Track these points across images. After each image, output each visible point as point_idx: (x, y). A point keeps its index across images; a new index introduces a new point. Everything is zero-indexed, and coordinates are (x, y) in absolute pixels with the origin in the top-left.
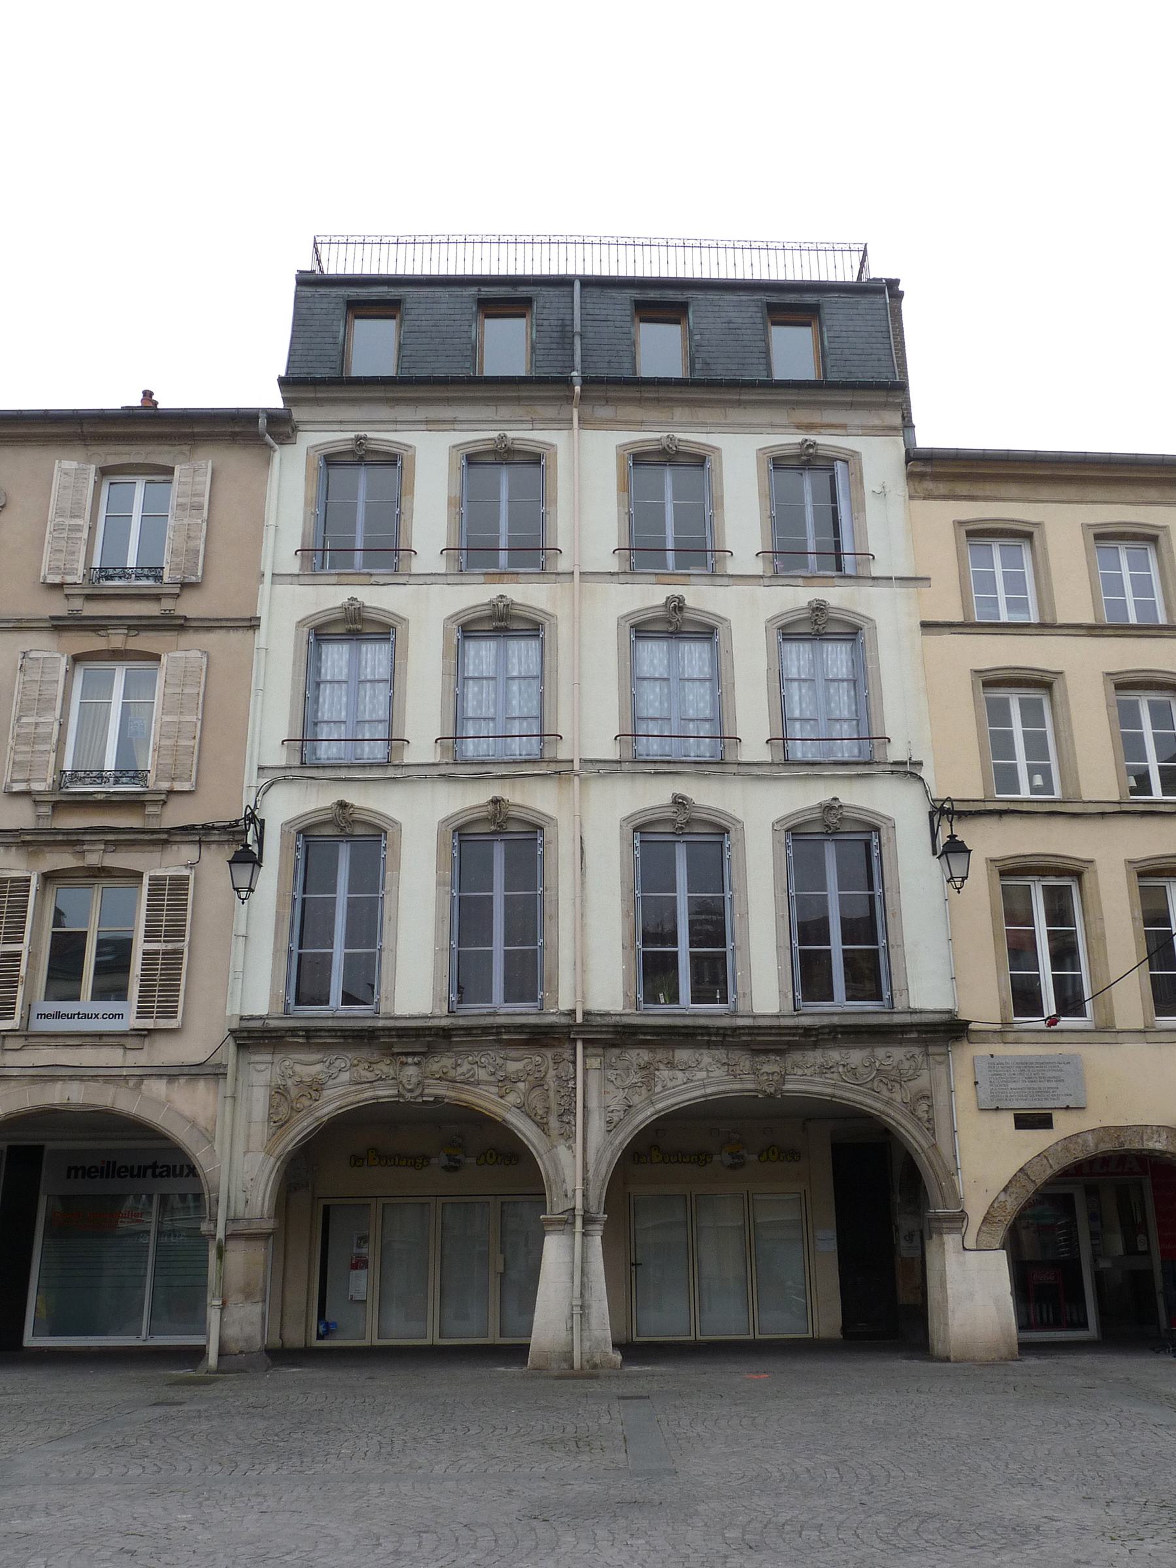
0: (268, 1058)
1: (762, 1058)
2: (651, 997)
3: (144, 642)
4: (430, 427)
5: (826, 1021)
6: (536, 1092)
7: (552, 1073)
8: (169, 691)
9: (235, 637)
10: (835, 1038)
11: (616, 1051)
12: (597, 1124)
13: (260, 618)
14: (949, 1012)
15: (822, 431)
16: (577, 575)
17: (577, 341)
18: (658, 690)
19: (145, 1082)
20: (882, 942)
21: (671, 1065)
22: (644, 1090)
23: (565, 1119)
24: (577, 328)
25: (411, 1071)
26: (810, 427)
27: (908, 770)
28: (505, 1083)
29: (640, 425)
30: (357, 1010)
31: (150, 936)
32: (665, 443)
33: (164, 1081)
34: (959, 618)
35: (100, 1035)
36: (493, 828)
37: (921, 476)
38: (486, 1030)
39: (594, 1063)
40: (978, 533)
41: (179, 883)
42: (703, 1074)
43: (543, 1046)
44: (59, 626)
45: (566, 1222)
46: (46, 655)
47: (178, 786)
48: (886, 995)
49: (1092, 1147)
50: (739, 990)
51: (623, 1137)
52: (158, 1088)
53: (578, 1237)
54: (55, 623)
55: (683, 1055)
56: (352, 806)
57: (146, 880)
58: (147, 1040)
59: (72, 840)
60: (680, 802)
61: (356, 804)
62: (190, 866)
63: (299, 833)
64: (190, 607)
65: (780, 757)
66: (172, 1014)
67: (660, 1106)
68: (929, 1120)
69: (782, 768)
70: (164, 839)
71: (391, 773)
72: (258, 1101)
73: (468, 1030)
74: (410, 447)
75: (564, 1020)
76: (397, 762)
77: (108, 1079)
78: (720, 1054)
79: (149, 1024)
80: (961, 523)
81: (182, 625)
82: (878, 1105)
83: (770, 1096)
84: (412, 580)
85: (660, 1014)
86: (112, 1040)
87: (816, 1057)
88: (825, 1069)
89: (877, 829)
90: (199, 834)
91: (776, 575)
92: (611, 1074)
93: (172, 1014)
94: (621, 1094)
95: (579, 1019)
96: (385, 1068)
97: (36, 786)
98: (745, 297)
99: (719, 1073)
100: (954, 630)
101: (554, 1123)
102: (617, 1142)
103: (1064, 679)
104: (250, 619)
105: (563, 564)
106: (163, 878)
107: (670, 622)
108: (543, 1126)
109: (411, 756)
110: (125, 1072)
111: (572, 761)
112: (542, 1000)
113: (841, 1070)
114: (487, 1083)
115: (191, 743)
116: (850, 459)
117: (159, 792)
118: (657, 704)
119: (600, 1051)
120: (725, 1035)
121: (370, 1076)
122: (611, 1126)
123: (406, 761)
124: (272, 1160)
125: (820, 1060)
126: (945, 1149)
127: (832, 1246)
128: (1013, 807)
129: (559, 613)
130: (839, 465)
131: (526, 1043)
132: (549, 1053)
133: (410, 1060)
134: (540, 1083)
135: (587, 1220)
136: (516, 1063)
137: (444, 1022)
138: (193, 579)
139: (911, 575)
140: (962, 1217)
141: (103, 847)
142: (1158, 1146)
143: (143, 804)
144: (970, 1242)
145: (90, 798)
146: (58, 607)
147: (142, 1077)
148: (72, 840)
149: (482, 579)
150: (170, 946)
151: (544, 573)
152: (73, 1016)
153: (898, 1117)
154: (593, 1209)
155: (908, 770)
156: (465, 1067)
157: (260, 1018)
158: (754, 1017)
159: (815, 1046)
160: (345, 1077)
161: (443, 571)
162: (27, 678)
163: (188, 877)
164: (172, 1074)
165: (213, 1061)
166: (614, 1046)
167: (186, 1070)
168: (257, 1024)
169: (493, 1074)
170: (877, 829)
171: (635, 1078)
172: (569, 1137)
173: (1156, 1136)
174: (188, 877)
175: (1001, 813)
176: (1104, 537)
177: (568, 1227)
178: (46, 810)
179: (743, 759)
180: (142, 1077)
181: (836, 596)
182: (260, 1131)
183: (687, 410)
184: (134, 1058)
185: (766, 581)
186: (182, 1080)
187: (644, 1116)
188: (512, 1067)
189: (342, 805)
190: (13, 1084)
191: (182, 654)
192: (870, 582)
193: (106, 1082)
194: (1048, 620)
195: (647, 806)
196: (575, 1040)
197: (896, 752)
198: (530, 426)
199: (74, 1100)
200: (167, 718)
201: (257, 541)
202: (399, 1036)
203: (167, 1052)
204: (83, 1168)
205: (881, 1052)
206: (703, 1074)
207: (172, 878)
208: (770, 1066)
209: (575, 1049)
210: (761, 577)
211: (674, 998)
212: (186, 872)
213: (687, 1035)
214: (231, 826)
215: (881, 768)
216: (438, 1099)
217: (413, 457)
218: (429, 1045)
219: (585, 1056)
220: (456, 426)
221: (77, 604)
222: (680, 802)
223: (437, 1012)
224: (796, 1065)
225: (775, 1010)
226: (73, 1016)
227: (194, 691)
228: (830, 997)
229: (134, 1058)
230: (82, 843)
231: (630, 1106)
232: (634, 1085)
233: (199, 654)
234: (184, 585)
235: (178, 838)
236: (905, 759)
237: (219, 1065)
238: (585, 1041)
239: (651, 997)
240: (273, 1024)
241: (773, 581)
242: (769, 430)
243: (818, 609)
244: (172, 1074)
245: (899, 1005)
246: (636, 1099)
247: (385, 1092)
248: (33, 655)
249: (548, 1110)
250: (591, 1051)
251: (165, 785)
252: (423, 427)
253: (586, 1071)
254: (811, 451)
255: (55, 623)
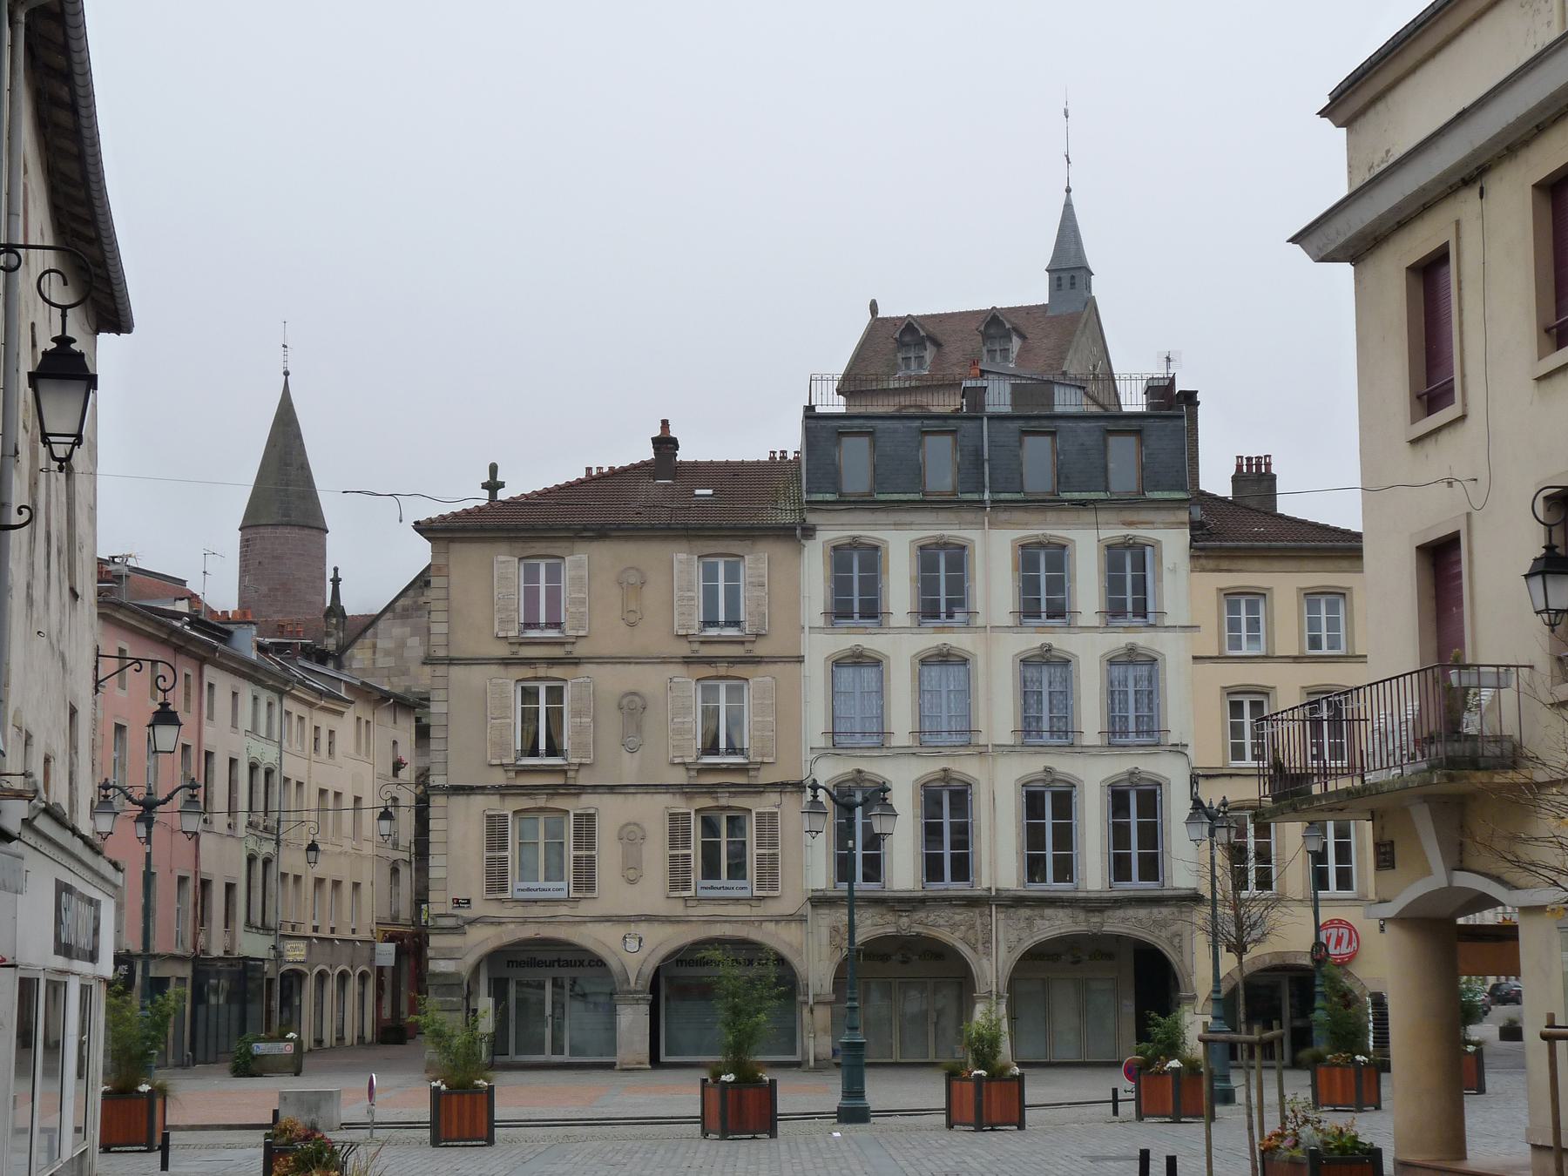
0: (827, 912)
1: (1091, 914)
2: (1031, 879)
3: (738, 670)
4: (897, 527)
5: (1126, 894)
6: (971, 931)
7: (979, 921)
8: (755, 702)
9: (789, 667)
10: (1131, 904)
11: (1013, 909)
12: (1003, 948)
13: (804, 656)
14: (1195, 889)
15: (1139, 526)
16: (988, 627)
17: (986, 466)
18: (1035, 697)
19: (764, 924)
20: (1160, 850)
21: (1042, 917)
22: (1028, 930)
23: (986, 945)
24: (986, 456)
25: (905, 920)
26: (1130, 524)
27: (1179, 749)
28: (954, 926)
29: (1025, 525)
30: (872, 885)
31: (759, 845)
32: (1042, 538)
33: (773, 923)
34: (1216, 654)
35: (738, 900)
36: (943, 784)
37: (1199, 557)
38: (944, 899)
39: (1002, 916)
40: (1231, 597)
41: (773, 815)
42: (1060, 922)
43: (973, 907)
44: (688, 661)
45: (986, 997)
46: (683, 680)
47: (766, 760)
48: (1161, 879)
49: (1268, 962)
50: (1080, 877)
51: (1017, 954)
52: (771, 927)
53: (994, 1003)
54: (686, 660)
55: (1049, 912)
56: (864, 772)
57: (754, 814)
58: (762, 902)
59: (711, 790)
60: (1048, 770)
61: (866, 770)
62: (778, 806)
63: (834, 786)
64: (761, 649)
65: (1106, 742)
66: (775, 888)
67: (1036, 939)
68: (1180, 947)
69: (1106, 749)
70: (759, 790)
71: (885, 752)
72: (825, 933)
73: (935, 899)
74: (885, 541)
75: (985, 893)
76: (887, 745)
77: (744, 922)
78: (1069, 911)
79: (763, 893)
80: (1221, 590)
81: (759, 661)
82: (1154, 940)
83: (1095, 934)
84: (891, 630)
85: (1036, 889)
86: (744, 902)
87: (1120, 913)
88: (1124, 920)
89: (1160, 785)
90: (780, 787)
91: (1107, 626)
92: (1009, 922)
93: (775, 888)
94: (1016, 933)
95: (993, 893)
96: (890, 917)
97: (688, 760)
98: (1093, 424)
99: (1068, 921)
100: (1212, 661)
101: (980, 947)
102: (1013, 958)
103: (1276, 692)
104: (798, 657)
105: (980, 621)
106: (764, 813)
107: (1044, 658)
108: (975, 949)
109: (895, 741)
110: (753, 919)
111: (987, 746)
112: (973, 882)
113: (1133, 920)
114: (943, 926)
115: (771, 733)
116: (1155, 545)
117: (756, 763)
118: (1035, 706)
119: (1005, 910)
120: (1072, 902)
121: (882, 922)
122: (1010, 949)
123: (893, 744)
124: (833, 965)
125: (1123, 915)
126: (1187, 961)
127: (1132, 1009)
128: (1238, 772)
129: (978, 653)
130: (1148, 549)
131: (965, 905)
132: (977, 911)
133: (904, 914)
134: (972, 927)
135: (999, 996)
136: (961, 916)
137: (920, 894)
138: (764, 632)
139: (1189, 624)
140: (1194, 997)
141: (728, 795)
142: (1304, 962)
143: (748, 770)
144: (1198, 1010)
145: (718, 767)
146: (684, 649)
147: (761, 922)
148: (711, 790)
149: (932, 630)
150: (771, 851)
151: (968, 626)
152: (720, 888)
153: (1164, 946)
154: (1001, 991)
155: (1179, 749)
156: (933, 917)
157: (822, 890)
158: (1087, 892)
159: (1120, 907)
160: (869, 922)
161: (909, 625)
162: (674, 694)
163: (777, 813)
164: (777, 920)
165: (800, 913)
166: (1013, 907)
167: (785, 918)
168: (820, 894)
169: (947, 921)
170: (1160, 785)
171: (1023, 924)
172: (989, 954)
173: (1303, 958)
174: (777, 813)
175: (1231, 775)
176: (1311, 596)
177: (987, 1000)
178: (693, 773)
179: (1085, 744)
180: (761, 922)
181: (1143, 639)
182: (826, 950)
183: (1054, 513)
184: (756, 911)
185: (1101, 630)
186: (783, 923)
187: (1027, 944)
188: (958, 918)
189: (859, 771)
190: (694, 924)
191: (760, 679)
192: (1164, 630)
193: (742, 924)
194: (1271, 654)
195: (1031, 772)
196: (991, 905)
197: (1173, 739)
198: (958, 527)
199: (727, 933)
200: (756, 719)
201: (797, 603)
202: (899, 902)
203: (773, 908)
204: (685, 961)
205: (1155, 910)
206: (1060, 922)
207: (769, 813)
208: (1095, 919)
209: (991, 908)
210: (1097, 627)
211: (1044, 880)
212: (776, 810)
213: (1052, 902)
214: (798, 784)
215: (1164, 748)
216: (918, 935)
217: (887, 549)
218: (913, 906)
219: (997, 912)
220: (913, 527)
221: (696, 646)
222: (1048, 770)
223: (916, 888)
224: (1109, 917)
225: (1099, 888)
226: (720, 888)
227: (770, 702)
228: (1129, 879)
229: (756, 911)
230: (717, 792)
231: (1020, 939)
232: (1023, 928)
233: (770, 679)
234: (757, 635)
235: (769, 790)
236: (1178, 742)
237: (802, 915)
238: (996, 905)
239: (1031, 879)
240: (830, 894)
241: (1105, 630)
242: (1106, 527)
243: (1132, 650)
244: (777, 920)
245: (1167, 885)
246: (1023, 936)
247: (891, 930)
248: (675, 680)
249: (977, 940)
250: (999, 910)
251: (759, 759)
252: (892, 527)
253: (997, 920)
254: (1131, 542)
255: (686, 660)
